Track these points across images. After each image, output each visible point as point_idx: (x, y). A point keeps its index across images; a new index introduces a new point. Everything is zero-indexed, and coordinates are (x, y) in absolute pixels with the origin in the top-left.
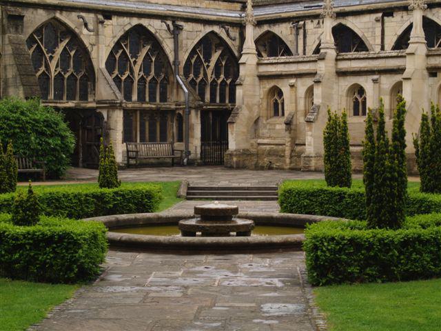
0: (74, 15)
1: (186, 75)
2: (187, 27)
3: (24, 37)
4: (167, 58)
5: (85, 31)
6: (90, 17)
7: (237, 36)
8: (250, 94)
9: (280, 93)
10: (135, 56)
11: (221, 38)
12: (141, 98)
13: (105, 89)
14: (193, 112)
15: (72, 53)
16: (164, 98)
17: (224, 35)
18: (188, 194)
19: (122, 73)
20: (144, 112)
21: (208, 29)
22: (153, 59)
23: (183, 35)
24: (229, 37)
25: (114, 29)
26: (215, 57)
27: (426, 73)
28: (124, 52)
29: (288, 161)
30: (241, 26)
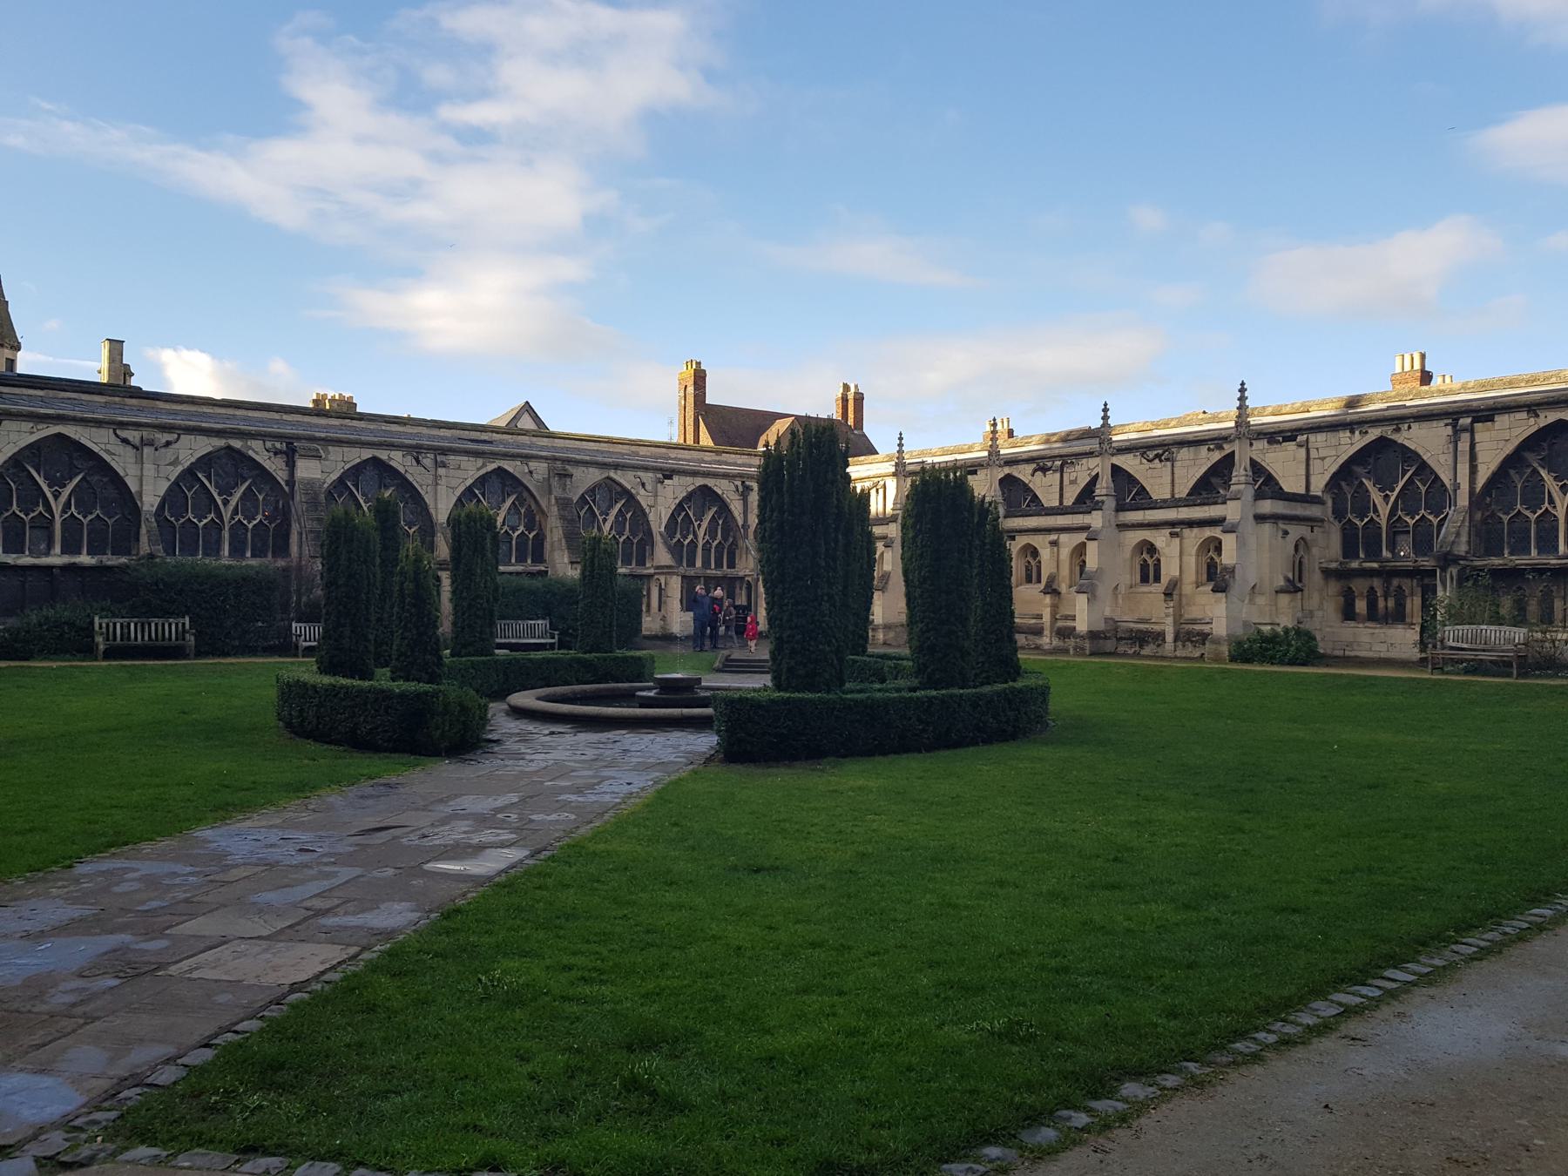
0: (630, 474)
4: (736, 521)
5: (642, 492)
6: (648, 477)
15: (628, 516)
16: (732, 565)
19: (685, 537)
22: (720, 522)
25: (676, 490)
28: (687, 514)
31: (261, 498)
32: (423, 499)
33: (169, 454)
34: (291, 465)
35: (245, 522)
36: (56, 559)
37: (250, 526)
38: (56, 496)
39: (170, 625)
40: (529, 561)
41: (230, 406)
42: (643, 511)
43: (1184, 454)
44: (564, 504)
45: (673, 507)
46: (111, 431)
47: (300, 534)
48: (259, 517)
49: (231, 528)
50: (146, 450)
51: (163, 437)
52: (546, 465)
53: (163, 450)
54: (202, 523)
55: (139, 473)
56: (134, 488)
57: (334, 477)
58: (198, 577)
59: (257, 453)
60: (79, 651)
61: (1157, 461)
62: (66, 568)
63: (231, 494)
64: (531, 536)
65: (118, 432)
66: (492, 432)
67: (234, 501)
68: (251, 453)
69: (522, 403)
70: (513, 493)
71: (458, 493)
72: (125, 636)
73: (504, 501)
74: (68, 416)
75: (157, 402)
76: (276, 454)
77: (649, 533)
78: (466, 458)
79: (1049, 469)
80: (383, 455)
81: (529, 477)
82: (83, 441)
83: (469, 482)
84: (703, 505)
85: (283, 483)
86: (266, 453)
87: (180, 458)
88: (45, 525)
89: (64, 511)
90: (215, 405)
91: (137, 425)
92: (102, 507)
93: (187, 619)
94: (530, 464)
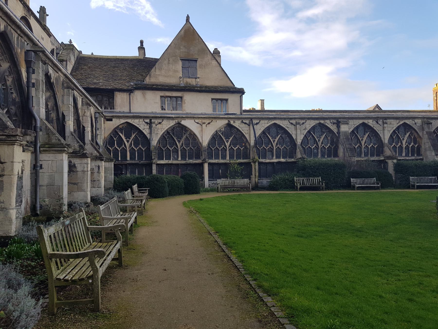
31: (329, 138)
32: (379, 136)
33: (303, 126)
34: (338, 127)
35: (325, 146)
36: (275, 160)
37: (326, 148)
38: (274, 141)
39: (315, 180)
40: (416, 155)
41: (308, 112)
44: (429, 133)
46: (288, 121)
47: (344, 149)
48: (329, 145)
49: (321, 148)
50: (298, 126)
51: (302, 122)
52: (421, 120)
53: (302, 125)
54: (313, 148)
55: (296, 133)
56: (294, 138)
57: (351, 130)
58: (322, 164)
59: (328, 124)
60: (291, 188)
62: (277, 163)
63: (320, 138)
64: (416, 146)
65: (290, 121)
66: (388, 112)
67: (321, 140)
68: (326, 124)
69: (375, 104)
70: (409, 131)
71: (391, 132)
72: (303, 183)
74: (277, 117)
75: (289, 113)
76: (334, 124)
78: (393, 120)
80: (366, 121)
82: (281, 125)
83: (395, 128)
85: (336, 133)
86: (331, 124)
87: (307, 128)
88: (271, 150)
89: (276, 146)
90: (304, 112)
91: (295, 118)
92: (285, 144)
93: (320, 177)
94: (415, 120)
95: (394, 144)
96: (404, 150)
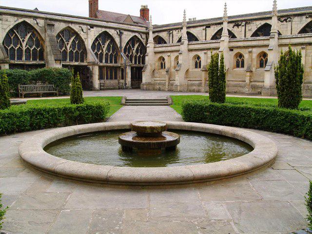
0: (77, 26)
1: (125, 53)
2: (125, 33)
3: (55, 34)
5: (82, 33)
6: (84, 27)
7: (145, 38)
8: (151, 59)
9: (164, 59)
10: (104, 44)
11: (138, 38)
12: (106, 62)
13: (91, 57)
14: (128, 67)
15: (77, 42)
16: (116, 62)
17: (140, 37)
18: (126, 103)
20: (107, 67)
21: (134, 34)
23: (123, 36)
24: (142, 38)
26: (136, 46)
27: (228, 49)
28: (99, 42)
29: (167, 87)
30: (147, 34)
40: (38, 60)
42: (82, 41)
43: (296, 19)
45: (94, 39)
61: (285, 22)
64: (38, 50)
69: (35, 8)
71: (7, 31)
73: (26, 35)
77: (85, 49)
78: (10, 17)
79: (240, 25)
81: (37, 25)
83: (11, 27)
84: (105, 39)
94: (37, 20)
95: (12, 45)
96: (24, 53)
